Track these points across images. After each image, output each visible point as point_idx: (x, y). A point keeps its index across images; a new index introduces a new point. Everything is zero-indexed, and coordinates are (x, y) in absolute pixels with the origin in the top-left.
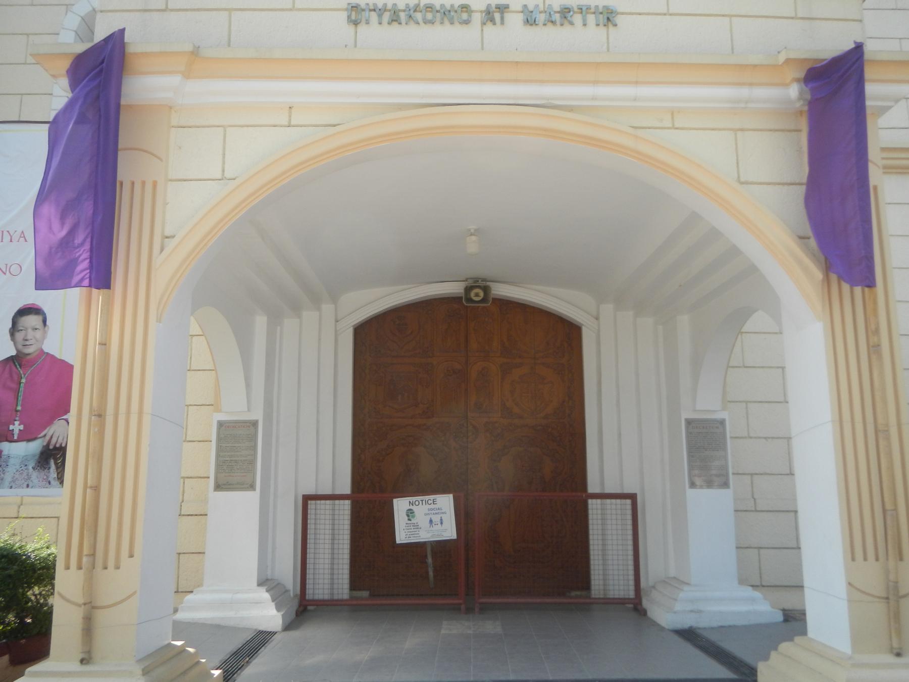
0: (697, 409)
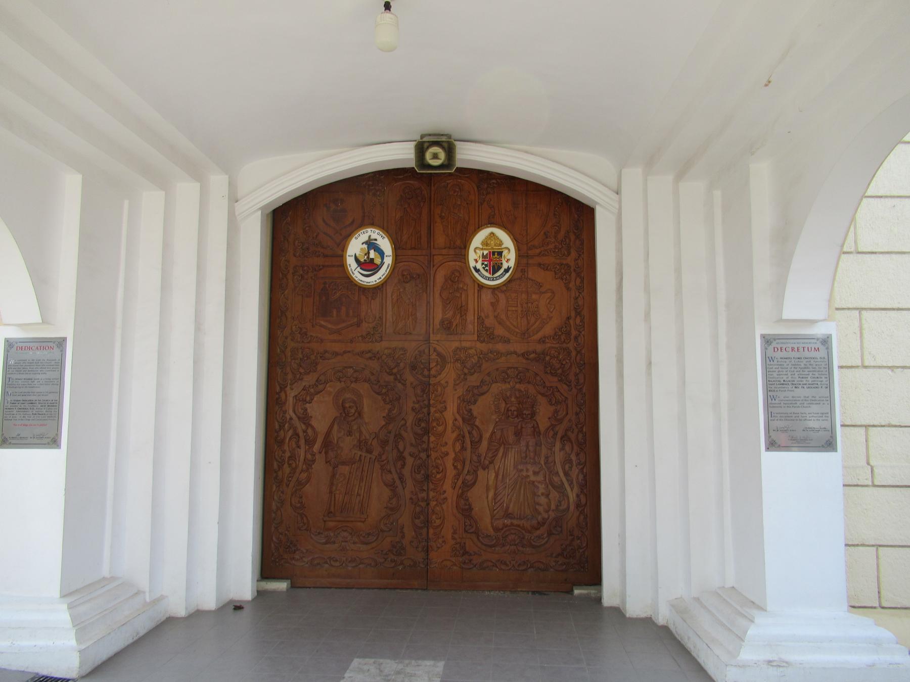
0: (784, 317)
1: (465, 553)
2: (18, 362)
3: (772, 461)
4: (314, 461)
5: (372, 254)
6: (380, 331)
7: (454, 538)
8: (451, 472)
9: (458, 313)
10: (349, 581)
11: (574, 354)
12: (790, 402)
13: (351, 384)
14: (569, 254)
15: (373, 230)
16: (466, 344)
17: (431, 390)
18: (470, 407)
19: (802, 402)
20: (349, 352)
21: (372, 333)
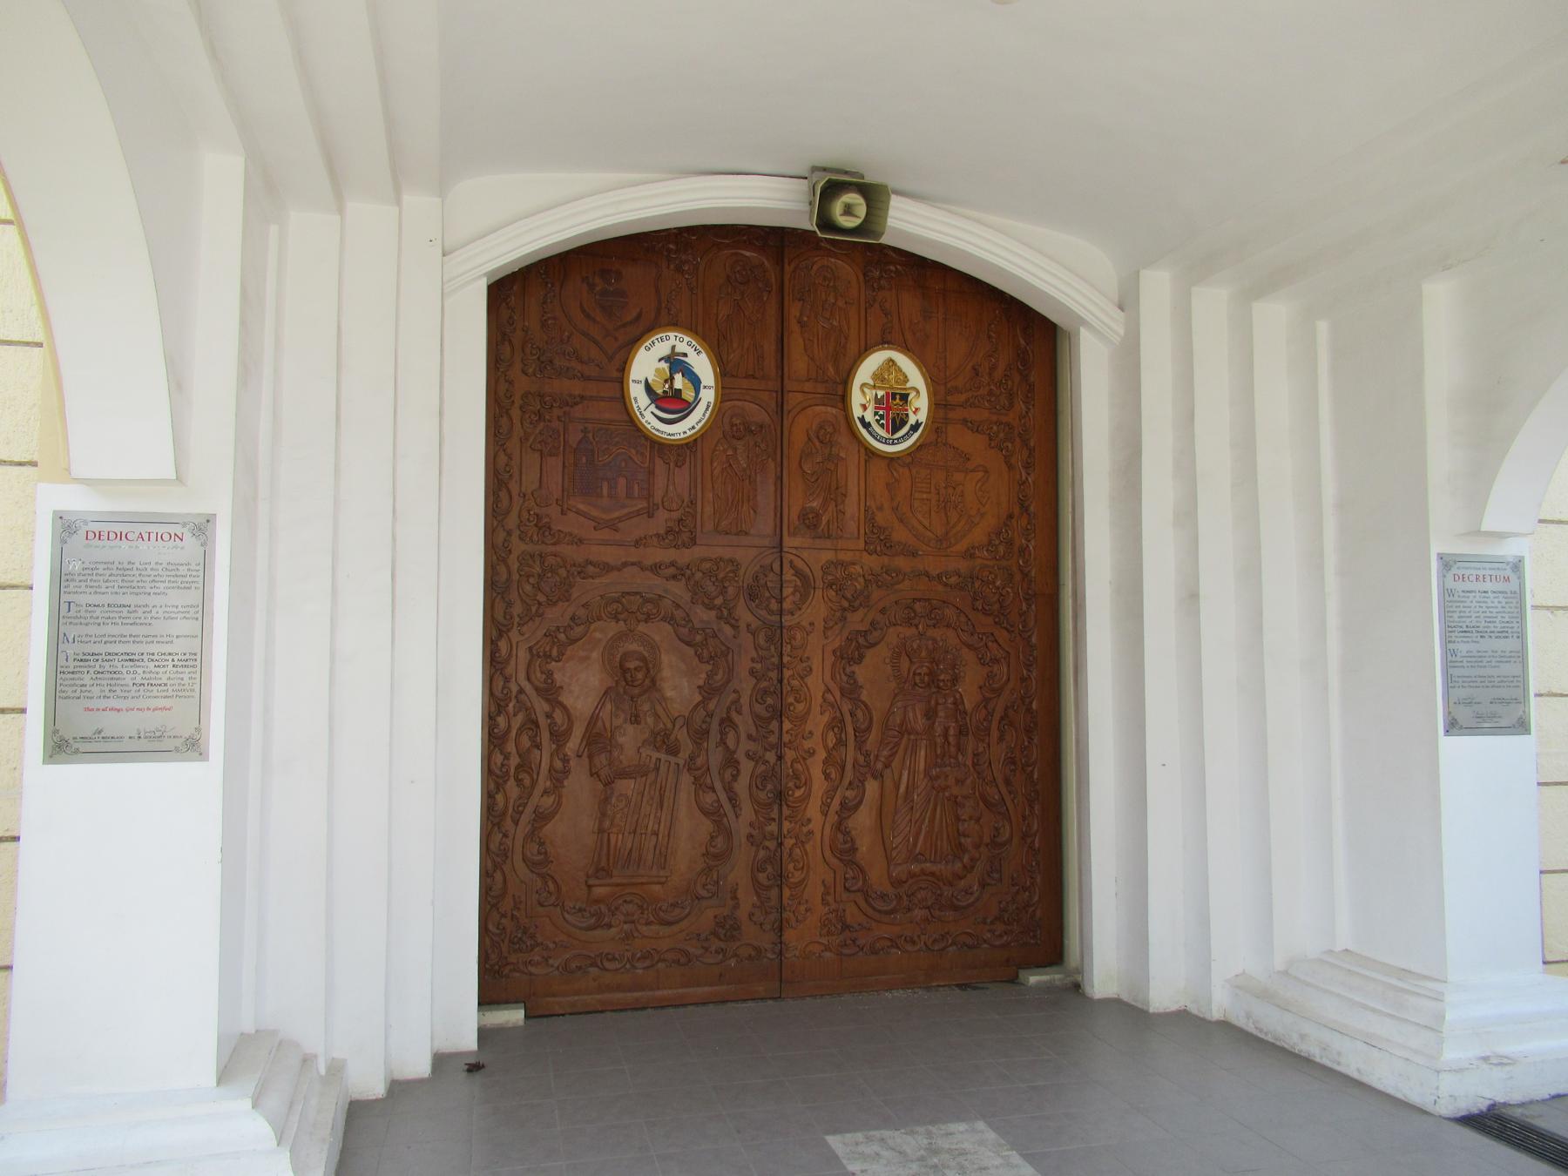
0: (1484, 528)
1: (846, 927)
2: (92, 566)
3: (1457, 752)
4: (566, 772)
5: (679, 382)
7: (825, 902)
8: (819, 785)
9: (832, 499)
10: (637, 994)
11: (1018, 577)
12: (1474, 659)
14: (1011, 405)
15: (680, 335)
16: (846, 557)
17: (785, 636)
18: (853, 668)
19: (1489, 660)
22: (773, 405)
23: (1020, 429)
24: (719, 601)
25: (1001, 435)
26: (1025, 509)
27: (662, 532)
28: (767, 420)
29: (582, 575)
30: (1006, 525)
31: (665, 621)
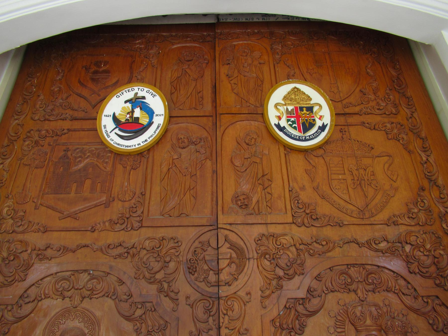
5: (138, 113)
6: (139, 212)
9: (260, 184)
13: (82, 301)
15: (141, 88)
17: (222, 307)
20: (86, 246)
21: (127, 216)
22: (210, 124)
23: (410, 126)
24: (159, 276)
25: (395, 131)
26: (433, 182)
27: (115, 217)
28: (205, 134)
29: (41, 257)
30: (419, 195)
31: (108, 296)
